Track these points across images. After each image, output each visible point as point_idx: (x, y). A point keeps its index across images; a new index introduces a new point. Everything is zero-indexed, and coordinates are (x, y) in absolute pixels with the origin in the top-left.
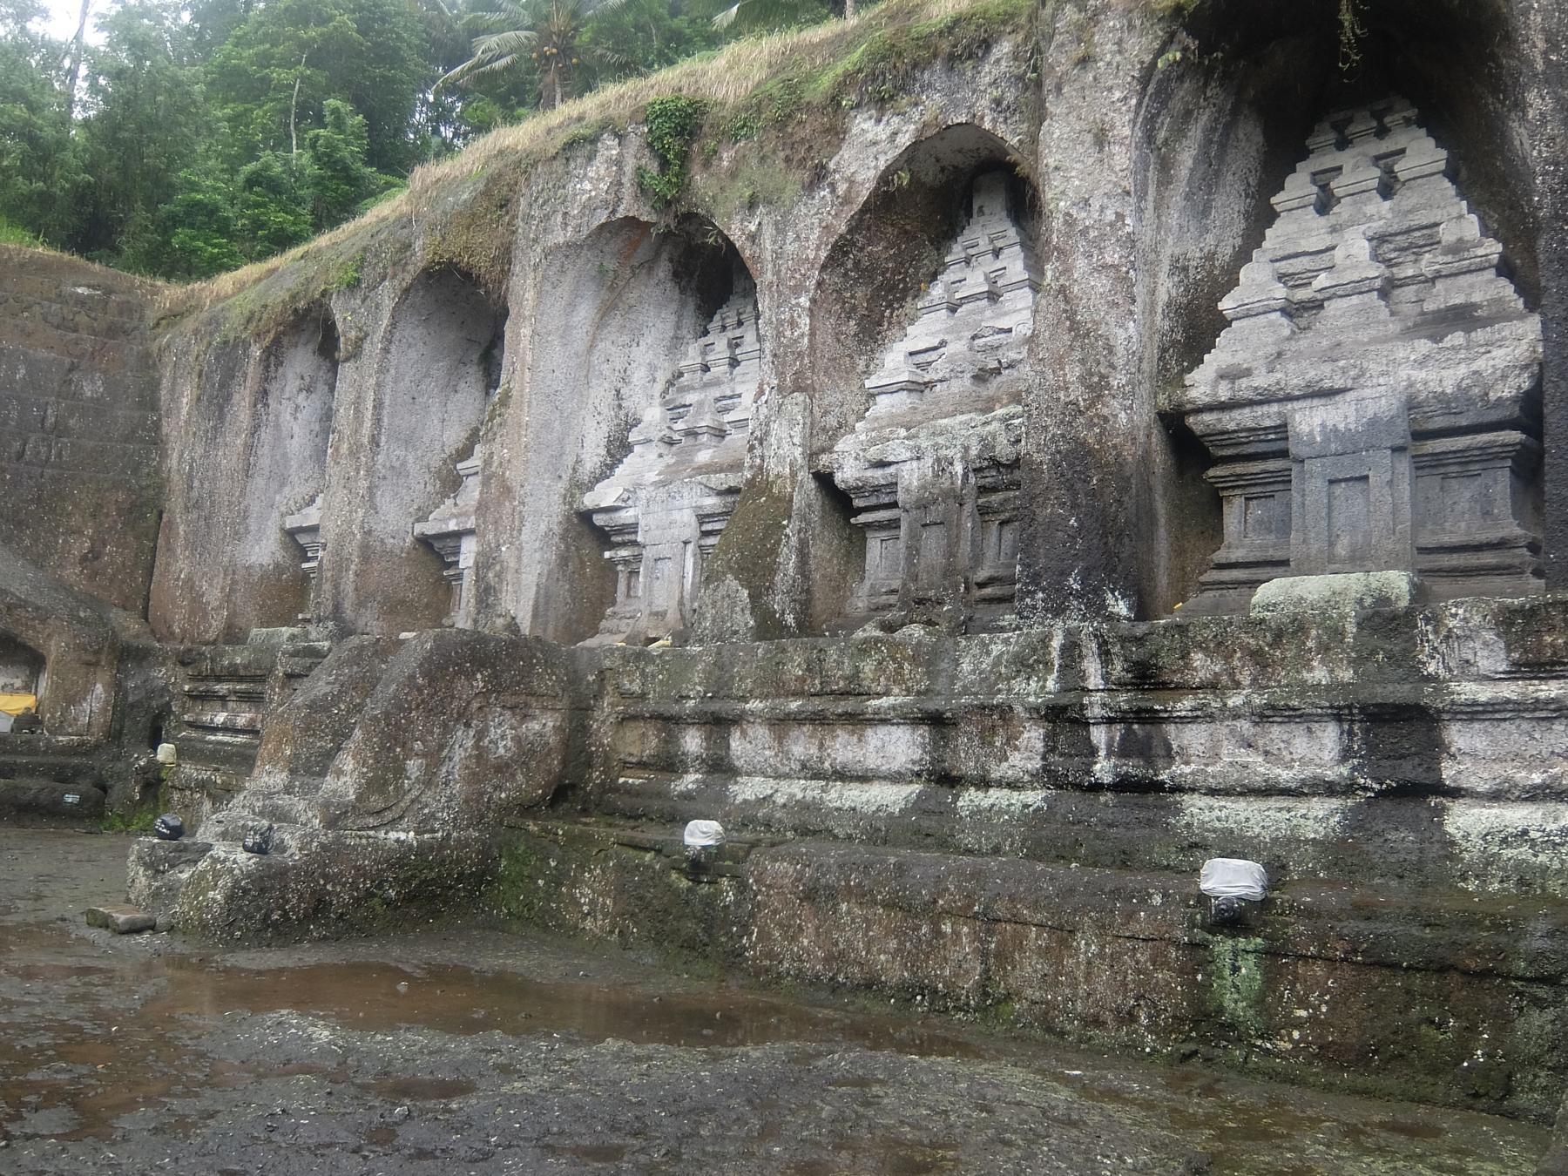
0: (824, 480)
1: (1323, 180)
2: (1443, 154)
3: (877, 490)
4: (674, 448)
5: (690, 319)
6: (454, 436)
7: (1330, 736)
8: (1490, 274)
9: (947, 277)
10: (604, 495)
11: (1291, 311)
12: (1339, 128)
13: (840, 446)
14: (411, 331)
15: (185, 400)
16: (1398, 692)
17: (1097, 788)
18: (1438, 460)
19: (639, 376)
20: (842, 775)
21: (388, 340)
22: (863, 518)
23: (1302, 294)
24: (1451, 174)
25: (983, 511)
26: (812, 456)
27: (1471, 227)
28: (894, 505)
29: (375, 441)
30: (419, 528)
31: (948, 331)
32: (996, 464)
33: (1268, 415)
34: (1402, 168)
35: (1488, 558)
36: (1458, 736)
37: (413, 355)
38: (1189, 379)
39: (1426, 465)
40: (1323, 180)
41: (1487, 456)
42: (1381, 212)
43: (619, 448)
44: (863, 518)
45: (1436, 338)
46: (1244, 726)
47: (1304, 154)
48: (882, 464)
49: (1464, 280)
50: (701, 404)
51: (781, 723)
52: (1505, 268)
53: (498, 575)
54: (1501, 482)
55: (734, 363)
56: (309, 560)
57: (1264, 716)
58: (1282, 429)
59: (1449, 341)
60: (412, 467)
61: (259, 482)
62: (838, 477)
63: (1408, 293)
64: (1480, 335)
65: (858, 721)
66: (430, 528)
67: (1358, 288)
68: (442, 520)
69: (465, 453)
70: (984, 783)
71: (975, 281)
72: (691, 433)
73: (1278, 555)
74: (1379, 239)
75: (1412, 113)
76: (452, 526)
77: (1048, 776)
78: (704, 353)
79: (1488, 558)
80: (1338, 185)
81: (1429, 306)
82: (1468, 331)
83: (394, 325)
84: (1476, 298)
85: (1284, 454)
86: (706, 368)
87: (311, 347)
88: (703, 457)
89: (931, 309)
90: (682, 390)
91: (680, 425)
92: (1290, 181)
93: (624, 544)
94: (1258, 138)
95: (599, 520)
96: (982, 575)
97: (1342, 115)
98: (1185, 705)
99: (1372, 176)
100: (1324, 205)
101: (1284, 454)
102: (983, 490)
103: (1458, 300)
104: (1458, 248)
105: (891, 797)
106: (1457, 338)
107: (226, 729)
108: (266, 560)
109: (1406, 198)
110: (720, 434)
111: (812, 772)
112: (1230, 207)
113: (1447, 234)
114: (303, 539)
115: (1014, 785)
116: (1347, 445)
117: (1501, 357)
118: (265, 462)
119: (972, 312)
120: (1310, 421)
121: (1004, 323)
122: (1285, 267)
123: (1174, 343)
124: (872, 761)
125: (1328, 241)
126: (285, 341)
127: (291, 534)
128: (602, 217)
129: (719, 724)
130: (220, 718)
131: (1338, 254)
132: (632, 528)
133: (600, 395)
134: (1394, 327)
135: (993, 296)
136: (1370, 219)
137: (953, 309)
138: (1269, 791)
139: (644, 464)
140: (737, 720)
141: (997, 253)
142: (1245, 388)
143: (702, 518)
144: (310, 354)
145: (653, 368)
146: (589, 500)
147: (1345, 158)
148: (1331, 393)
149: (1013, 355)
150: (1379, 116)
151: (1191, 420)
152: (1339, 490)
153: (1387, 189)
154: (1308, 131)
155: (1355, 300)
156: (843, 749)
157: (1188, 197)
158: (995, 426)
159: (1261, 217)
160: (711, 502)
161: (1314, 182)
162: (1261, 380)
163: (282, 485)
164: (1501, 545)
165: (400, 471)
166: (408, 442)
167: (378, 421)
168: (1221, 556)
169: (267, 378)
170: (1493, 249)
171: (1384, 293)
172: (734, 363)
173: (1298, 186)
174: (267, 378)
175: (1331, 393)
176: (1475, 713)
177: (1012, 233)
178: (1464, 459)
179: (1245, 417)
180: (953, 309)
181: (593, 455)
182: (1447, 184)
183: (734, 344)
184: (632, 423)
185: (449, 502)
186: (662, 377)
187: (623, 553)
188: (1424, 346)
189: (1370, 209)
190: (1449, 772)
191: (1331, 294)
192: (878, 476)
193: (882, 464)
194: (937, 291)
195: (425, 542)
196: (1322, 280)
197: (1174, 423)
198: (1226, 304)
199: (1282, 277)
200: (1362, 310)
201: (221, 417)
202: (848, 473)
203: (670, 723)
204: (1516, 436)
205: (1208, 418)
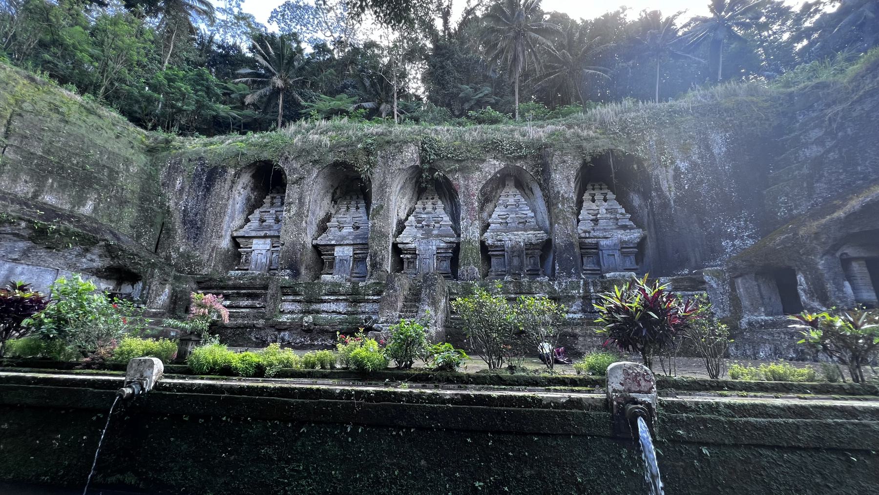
0: (482, 243)
3: (497, 246)
6: (322, 214)
9: (502, 198)
12: (593, 186)
15: (178, 182)
25: (527, 254)
27: (623, 211)
28: (504, 250)
30: (315, 242)
32: (531, 244)
33: (594, 241)
39: (623, 253)
40: (593, 196)
41: (631, 253)
52: (630, 219)
56: (241, 248)
58: (597, 244)
66: (320, 241)
71: (511, 200)
76: (333, 242)
77: (583, 311)
80: (596, 198)
83: (317, 177)
85: (596, 249)
87: (251, 174)
88: (435, 232)
93: (407, 254)
95: (400, 246)
100: (593, 201)
102: (526, 249)
106: (628, 231)
108: (225, 246)
115: (574, 313)
116: (609, 248)
117: (636, 235)
118: (229, 211)
120: (603, 242)
126: (243, 170)
132: (415, 249)
144: (249, 177)
145: (406, 206)
153: (605, 200)
160: (442, 245)
163: (233, 220)
165: (311, 223)
168: (585, 268)
169: (233, 182)
170: (629, 216)
172: (434, 209)
174: (233, 182)
179: (589, 240)
188: (623, 232)
193: (501, 241)
195: (316, 247)
202: (490, 242)
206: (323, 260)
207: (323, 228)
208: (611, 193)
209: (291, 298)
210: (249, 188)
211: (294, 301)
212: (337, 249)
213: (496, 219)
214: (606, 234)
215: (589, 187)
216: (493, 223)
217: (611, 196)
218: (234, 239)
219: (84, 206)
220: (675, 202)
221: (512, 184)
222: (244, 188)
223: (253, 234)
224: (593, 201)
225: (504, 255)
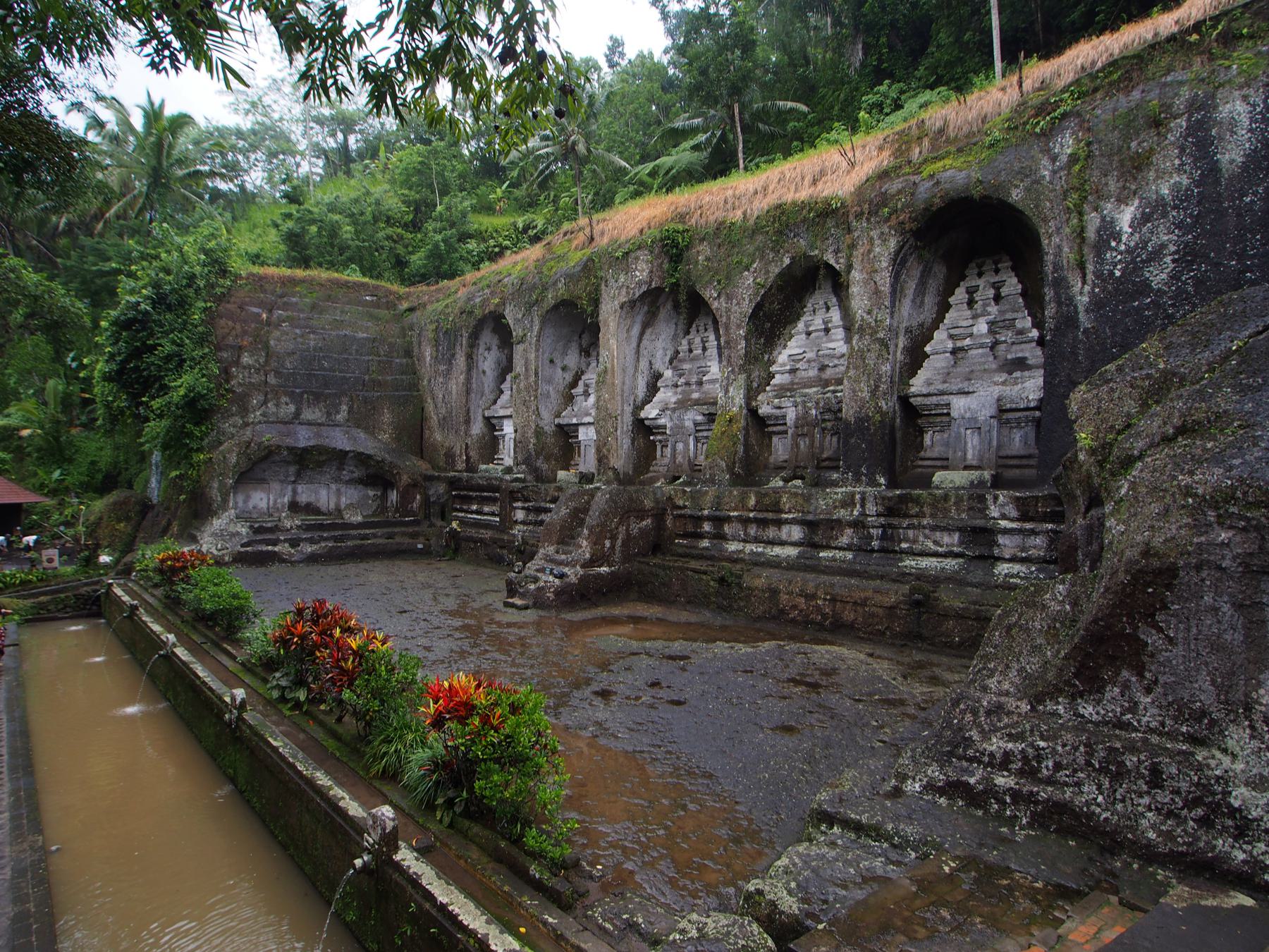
1: (971, 292)
2: (1020, 286)
3: (777, 418)
4: (679, 389)
5: (681, 326)
6: (569, 377)
7: (956, 536)
8: (1034, 344)
9: (803, 319)
10: (650, 412)
11: (954, 352)
12: (980, 266)
13: (760, 398)
14: (549, 331)
16: (979, 522)
17: (873, 551)
18: (1008, 421)
19: (659, 354)
20: (772, 543)
21: (539, 336)
22: (771, 429)
23: (959, 344)
24: (1024, 294)
26: (748, 404)
27: (1028, 322)
29: (536, 382)
30: (557, 421)
31: (805, 346)
34: (1004, 291)
35: (1025, 462)
36: (1001, 540)
37: (549, 341)
38: (911, 382)
40: (971, 292)
42: (993, 309)
43: (653, 389)
44: (771, 429)
45: (1010, 373)
46: (927, 531)
47: (963, 278)
48: (780, 408)
49: (1023, 346)
50: (690, 370)
51: (745, 522)
53: (609, 451)
54: (1030, 430)
55: (704, 349)
57: (934, 528)
58: (948, 405)
59: (1014, 375)
60: (552, 392)
61: (473, 395)
62: (760, 411)
63: (1002, 347)
64: (1026, 373)
65: (779, 523)
66: (562, 421)
67: (982, 346)
68: (568, 418)
69: (574, 384)
70: (828, 547)
71: (818, 323)
72: (687, 384)
73: (945, 456)
74: (991, 324)
75: (1009, 264)
76: (574, 421)
78: (689, 344)
79: (1025, 462)
80: (977, 296)
81: (1009, 357)
82: (1022, 371)
84: (1027, 355)
86: (691, 351)
89: (799, 333)
90: (680, 361)
91: (682, 380)
92: (957, 291)
94: (944, 270)
96: (825, 456)
97: (979, 261)
98: (906, 523)
99: (991, 293)
101: (948, 414)
103: (1020, 355)
104: (1021, 332)
105: (792, 552)
106: (1017, 374)
107: (477, 512)
109: (1004, 305)
110: (700, 383)
111: (757, 540)
112: (930, 301)
113: (1019, 324)
114: (494, 421)
115: (840, 549)
119: (817, 338)
121: (831, 345)
122: (953, 332)
123: (905, 364)
124: (784, 537)
125: (971, 322)
127: (488, 420)
128: (644, 288)
129: (719, 521)
130: (474, 507)
131: (975, 329)
133: (643, 364)
134: (994, 366)
135: (827, 330)
136: (989, 314)
137: (809, 334)
138: (936, 555)
139: (665, 395)
140: (728, 519)
141: (828, 309)
142: (932, 389)
143: (696, 424)
145: (665, 350)
146: (643, 415)
147: (981, 282)
148: (968, 393)
149: (836, 362)
150: (996, 263)
151: (912, 400)
152: (969, 432)
153: (997, 298)
154: (966, 266)
155: (980, 351)
156: (771, 532)
157: (913, 301)
158: (829, 395)
159: (944, 307)
160: (700, 418)
161: (968, 292)
162: (941, 387)
164: (1029, 457)
165: (548, 396)
166: (549, 382)
167: (536, 374)
170: (1035, 333)
171: (992, 348)
172: (704, 349)
173: (960, 294)
175: (968, 393)
176: (1006, 531)
177: (834, 300)
178: (1018, 421)
179: (934, 400)
180: (809, 334)
181: (641, 391)
182: (1021, 300)
183: (704, 342)
184: (658, 376)
185: (569, 408)
186: (669, 353)
187: (659, 437)
188: (1004, 376)
189: (989, 309)
190: (996, 552)
191: (970, 348)
192: (777, 412)
193: (780, 408)
194: (801, 326)
195: (559, 426)
196: (967, 342)
197: (904, 400)
198: (928, 349)
199: (951, 337)
200: (982, 355)
201: (450, 363)
202: (764, 410)
203: (699, 520)
204: (1037, 414)
205: (919, 399)
206: (571, 444)
207: (569, 399)
208: (1015, 280)
209: (519, 504)
210: (495, 348)
211: (523, 508)
212: (581, 430)
213: (784, 365)
214: (965, 386)
215: (972, 270)
216: (778, 372)
217: (1012, 285)
218: (488, 420)
219: (338, 412)
220: (1087, 311)
221: (828, 286)
222: (489, 349)
223: (502, 413)
224: (971, 303)
225: (786, 432)
